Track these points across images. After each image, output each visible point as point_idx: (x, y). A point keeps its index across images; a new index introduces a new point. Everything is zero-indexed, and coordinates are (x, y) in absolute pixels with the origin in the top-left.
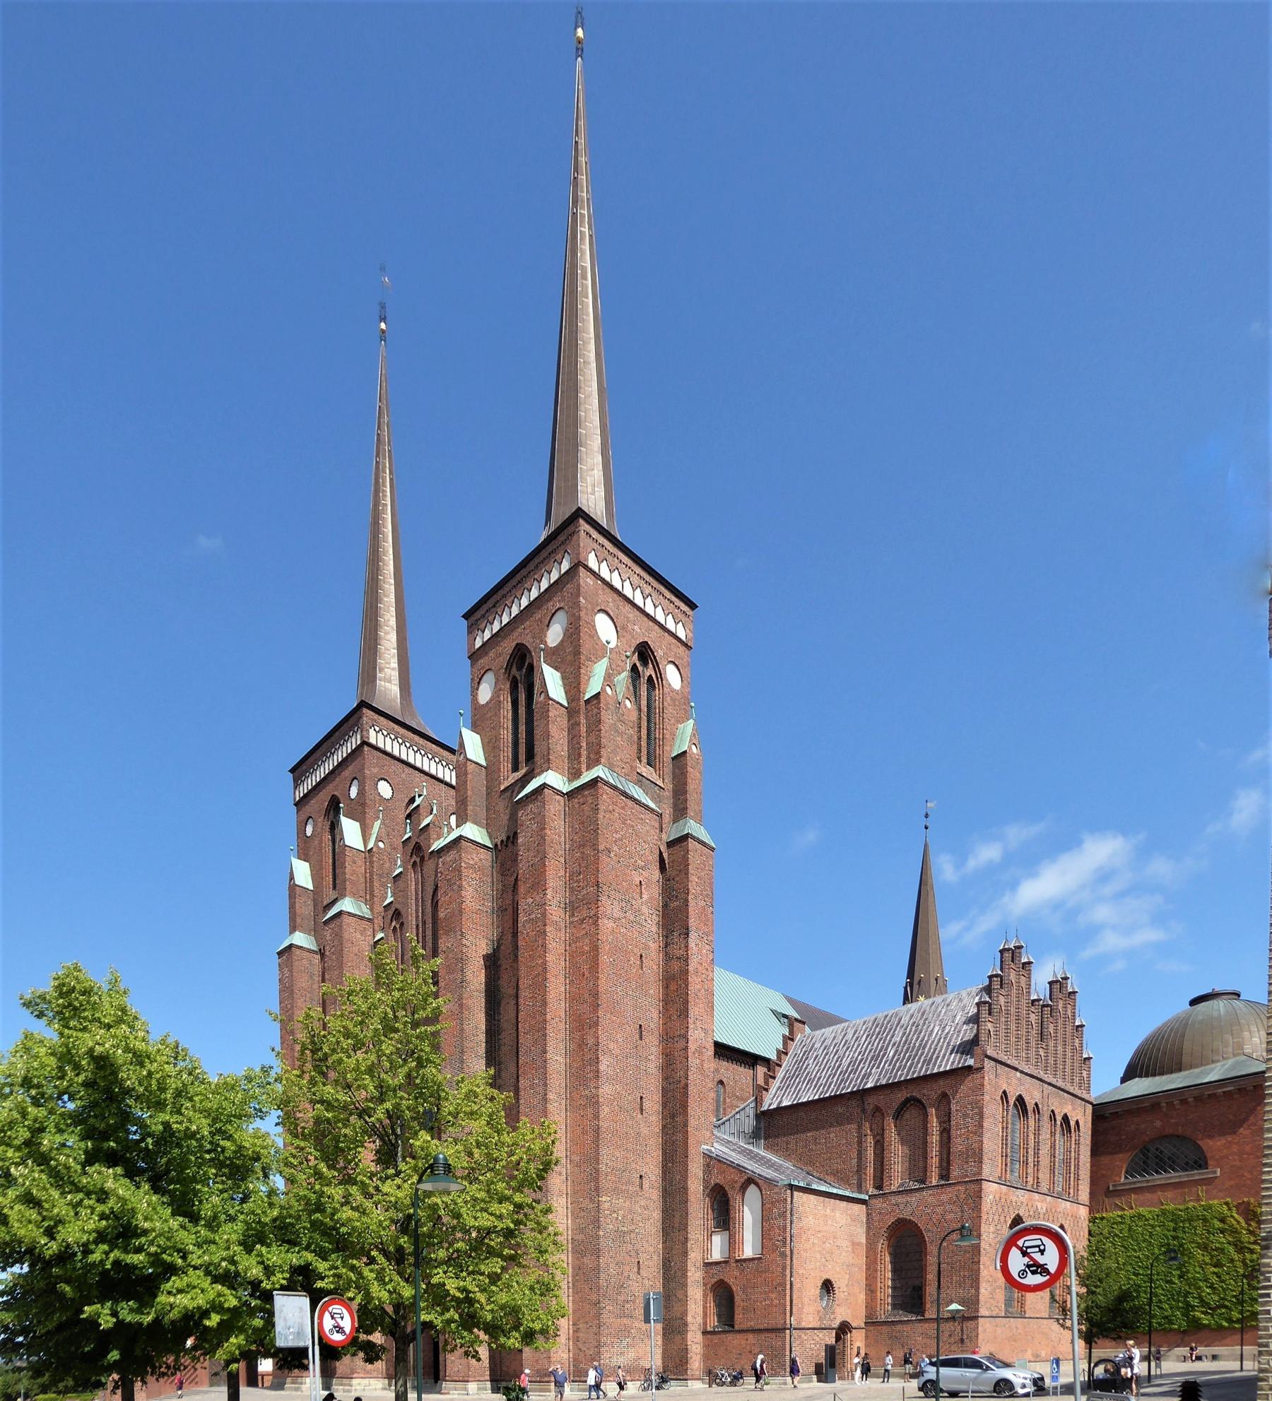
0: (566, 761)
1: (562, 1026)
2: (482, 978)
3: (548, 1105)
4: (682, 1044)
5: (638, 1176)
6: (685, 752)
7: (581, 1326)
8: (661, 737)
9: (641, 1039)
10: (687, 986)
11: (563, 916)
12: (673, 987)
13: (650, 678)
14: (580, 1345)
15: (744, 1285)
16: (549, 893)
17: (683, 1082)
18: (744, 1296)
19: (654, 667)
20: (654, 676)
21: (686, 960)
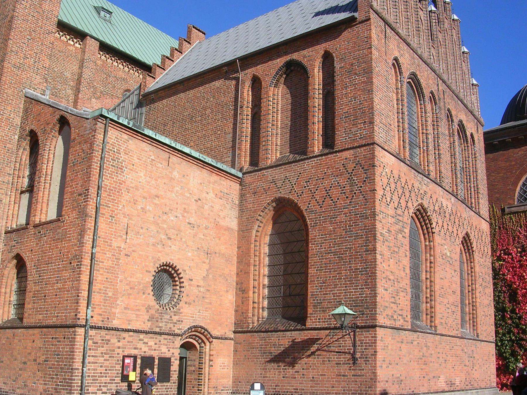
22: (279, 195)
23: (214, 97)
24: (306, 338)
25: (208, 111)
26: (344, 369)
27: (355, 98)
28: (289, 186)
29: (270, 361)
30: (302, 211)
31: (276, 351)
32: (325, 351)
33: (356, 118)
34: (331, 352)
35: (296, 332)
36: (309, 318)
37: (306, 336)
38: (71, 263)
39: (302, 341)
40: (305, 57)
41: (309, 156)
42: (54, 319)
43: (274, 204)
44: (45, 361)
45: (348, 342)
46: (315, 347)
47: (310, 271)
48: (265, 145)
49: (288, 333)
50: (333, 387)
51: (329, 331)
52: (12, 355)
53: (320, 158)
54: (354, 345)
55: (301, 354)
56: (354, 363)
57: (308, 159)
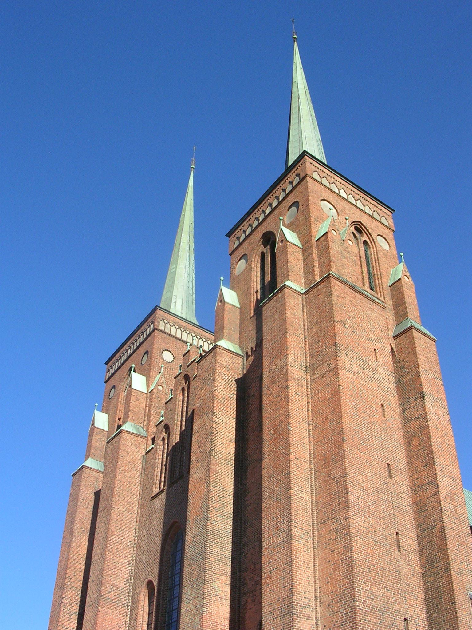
0: (303, 277)
1: (307, 466)
2: (232, 449)
3: (293, 541)
4: (431, 491)
5: (403, 619)
6: (400, 279)
8: (379, 273)
9: (390, 477)
10: (429, 438)
11: (304, 376)
12: (415, 442)
13: (365, 242)
16: (291, 359)
17: (438, 528)
19: (366, 234)
20: (368, 241)
21: (426, 417)
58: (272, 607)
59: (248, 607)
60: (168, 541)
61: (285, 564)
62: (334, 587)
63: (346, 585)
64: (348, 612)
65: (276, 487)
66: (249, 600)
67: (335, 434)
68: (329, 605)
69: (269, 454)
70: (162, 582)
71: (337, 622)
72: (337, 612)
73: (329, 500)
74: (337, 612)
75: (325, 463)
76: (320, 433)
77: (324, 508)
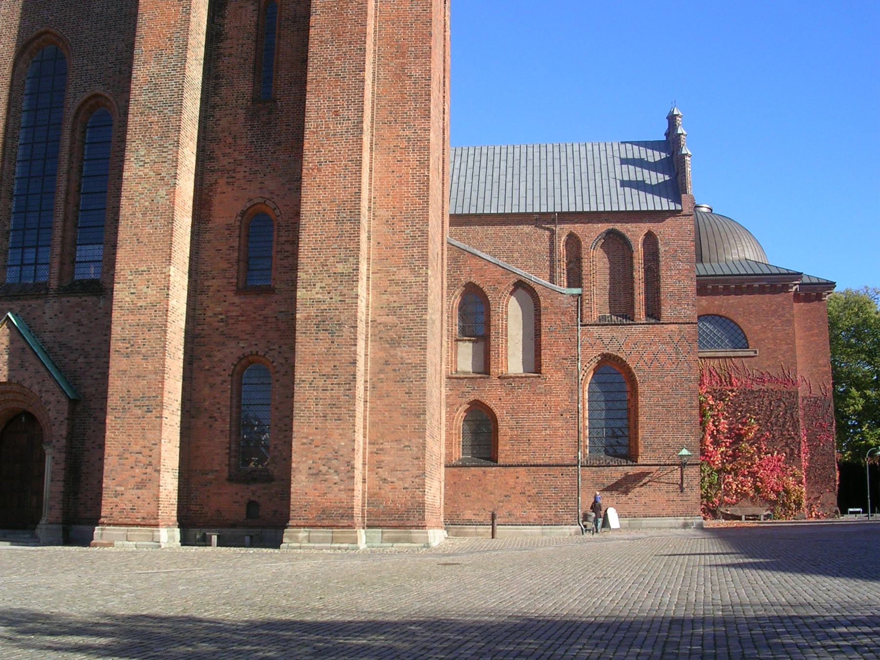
7: (387, 446)
14: (386, 475)
15: (512, 409)
18: (513, 423)
22: (606, 351)
23: (523, 242)
24: (637, 472)
25: (516, 255)
26: (672, 496)
27: (679, 281)
28: (616, 344)
29: (603, 490)
30: (630, 369)
31: (608, 483)
32: (656, 482)
33: (681, 298)
34: (661, 483)
35: (628, 467)
36: (640, 457)
37: (638, 470)
38: (562, 415)
39: (634, 475)
40: (628, 230)
41: (636, 322)
42: (547, 460)
43: (600, 358)
44: (537, 493)
45: (677, 474)
46: (647, 479)
47: (640, 419)
48: (588, 303)
49: (620, 468)
50: (663, 510)
51: (659, 467)
52: (485, 490)
53: (647, 326)
54: (682, 479)
55: (633, 485)
56: (682, 491)
57: (635, 324)
58: (321, 207)
59: (219, 190)
60: (25, 55)
61: (350, 161)
62: (397, 203)
63: (416, 204)
64: (417, 235)
65: (337, 59)
66: (222, 181)
67: (419, 22)
68: (387, 221)
69: (325, 12)
70: (12, 114)
71: (399, 242)
72: (399, 232)
73: (399, 99)
74: (399, 232)
75: (397, 52)
76: (392, 11)
77: (389, 106)
